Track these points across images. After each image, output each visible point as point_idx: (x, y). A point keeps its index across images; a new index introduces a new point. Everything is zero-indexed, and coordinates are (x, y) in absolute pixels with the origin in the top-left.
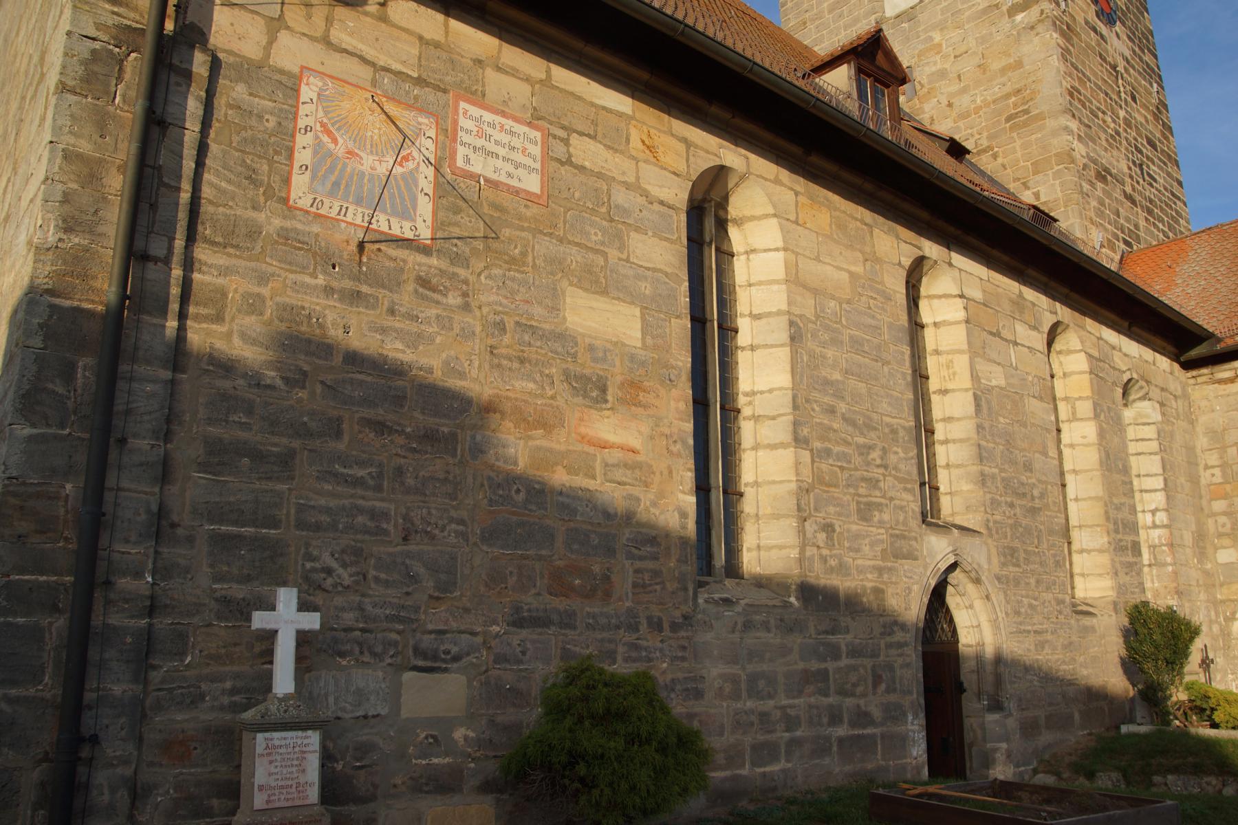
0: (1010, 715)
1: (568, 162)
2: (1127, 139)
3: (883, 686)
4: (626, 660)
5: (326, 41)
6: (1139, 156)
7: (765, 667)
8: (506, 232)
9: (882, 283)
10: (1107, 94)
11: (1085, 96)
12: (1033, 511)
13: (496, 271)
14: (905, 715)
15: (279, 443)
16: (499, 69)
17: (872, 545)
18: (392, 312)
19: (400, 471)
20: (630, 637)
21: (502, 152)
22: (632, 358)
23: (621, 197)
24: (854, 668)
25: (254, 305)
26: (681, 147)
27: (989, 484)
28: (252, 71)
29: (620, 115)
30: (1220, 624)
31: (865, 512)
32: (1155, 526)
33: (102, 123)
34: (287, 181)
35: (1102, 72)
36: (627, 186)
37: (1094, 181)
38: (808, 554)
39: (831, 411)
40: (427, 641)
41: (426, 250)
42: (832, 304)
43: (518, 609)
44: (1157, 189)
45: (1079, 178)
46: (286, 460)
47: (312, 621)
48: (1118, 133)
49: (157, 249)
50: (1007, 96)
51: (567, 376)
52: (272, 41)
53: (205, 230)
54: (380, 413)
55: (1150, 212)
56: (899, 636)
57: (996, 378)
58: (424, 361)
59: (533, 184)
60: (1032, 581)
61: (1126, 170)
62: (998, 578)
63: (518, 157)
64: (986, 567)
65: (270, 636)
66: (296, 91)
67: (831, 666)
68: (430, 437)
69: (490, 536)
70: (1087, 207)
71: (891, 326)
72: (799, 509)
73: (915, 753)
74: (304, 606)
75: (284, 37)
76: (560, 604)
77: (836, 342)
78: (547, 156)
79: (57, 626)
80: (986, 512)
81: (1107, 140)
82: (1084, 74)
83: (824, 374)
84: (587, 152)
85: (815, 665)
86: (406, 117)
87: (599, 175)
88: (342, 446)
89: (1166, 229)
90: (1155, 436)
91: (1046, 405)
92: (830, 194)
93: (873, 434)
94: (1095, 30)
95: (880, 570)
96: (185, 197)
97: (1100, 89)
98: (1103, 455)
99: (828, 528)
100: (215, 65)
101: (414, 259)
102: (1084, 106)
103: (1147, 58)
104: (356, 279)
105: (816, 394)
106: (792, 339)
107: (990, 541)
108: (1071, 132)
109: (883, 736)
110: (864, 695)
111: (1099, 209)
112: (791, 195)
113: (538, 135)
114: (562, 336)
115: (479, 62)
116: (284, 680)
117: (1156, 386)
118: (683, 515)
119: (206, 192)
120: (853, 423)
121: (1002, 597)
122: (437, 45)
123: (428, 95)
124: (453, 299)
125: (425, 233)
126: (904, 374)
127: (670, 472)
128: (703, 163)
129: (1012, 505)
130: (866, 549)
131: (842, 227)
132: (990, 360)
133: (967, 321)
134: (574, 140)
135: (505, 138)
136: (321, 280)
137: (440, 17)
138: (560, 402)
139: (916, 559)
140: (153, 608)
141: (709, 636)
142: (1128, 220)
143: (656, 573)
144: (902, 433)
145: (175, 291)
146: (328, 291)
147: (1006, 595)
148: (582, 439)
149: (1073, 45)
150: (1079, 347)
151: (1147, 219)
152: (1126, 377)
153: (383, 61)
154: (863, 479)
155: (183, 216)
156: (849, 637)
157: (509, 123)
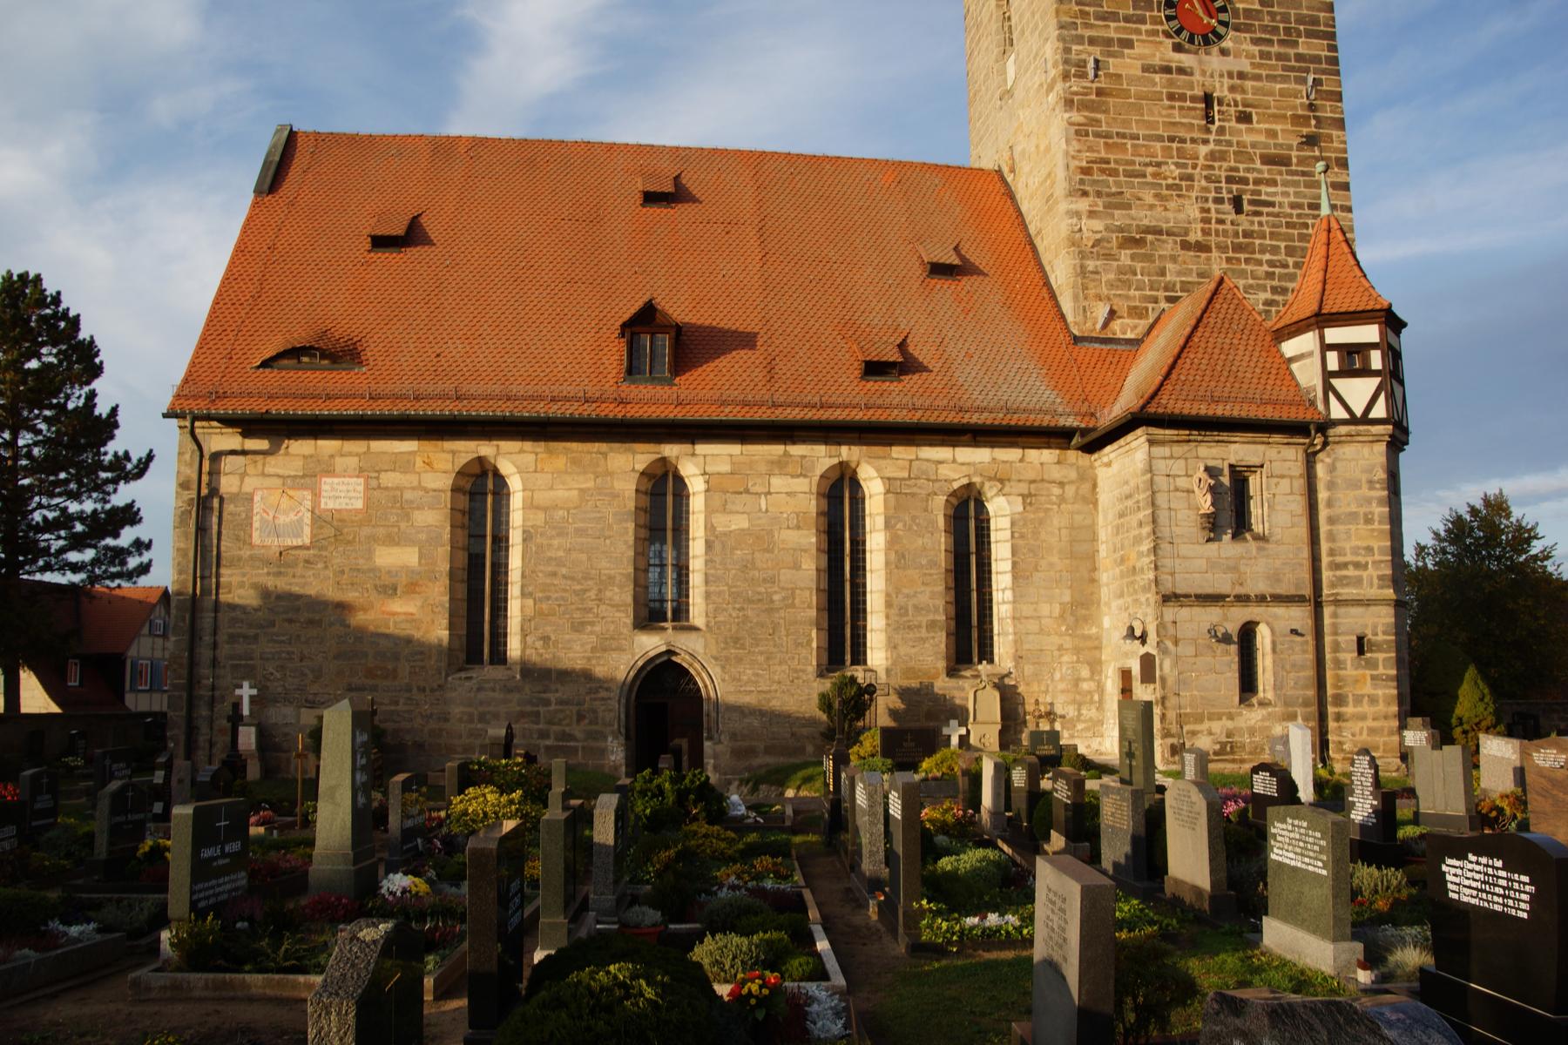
0: (720, 742)
1: (379, 487)
2: (1207, 178)
3: (587, 721)
4: (405, 704)
5: (263, 475)
6: (1234, 187)
7: (491, 709)
8: (345, 530)
9: (612, 487)
10: (1171, 139)
11: (1116, 162)
12: (770, 611)
13: (341, 549)
14: (605, 738)
15: (252, 632)
16: (342, 455)
17: (582, 645)
18: (294, 576)
19: (298, 636)
20: (408, 695)
21: (343, 495)
22: (413, 572)
23: (408, 495)
24: (562, 711)
25: (241, 585)
26: (450, 457)
27: (714, 598)
28: (235, 497)
29: (410, 453)
30: (1099, 682)
31: (578, 627)
32: (1004, 602)
33: (186, 535)
34: (251, 536)
35: (1169, 116)
36: (413, 489)
37: (1115, 251)
38: (528, 652)
39: (554, 574)
40: (310, 697)
41: (308, 548)
42: (561, 512)
43: (350, 685)
44: (1268, 214)
45: (1083, 258)
46: (256, 637)
47: (254, 692)
48: (1190, 178)
49: (207, 574)
50: (1045, 180)
51: (376, 586)
52: (242, 481)
53: (223, 562)
54: (290, 615)
55: (1238, 248)
56: (603, 694)
57: (739, 523)
58: (308, 593)
59: (359, 504)
60: (761, 659)
61: (1198, 215)
62: (716, 659)
63: (352, 494)
64: (702, 651)
65: (241, 697)
66: (252, 499)
67: (542, 709)
68: (311, 622)
69: (336, 657)
70: (1091, 285)
71: (615, 514)
72: (522, 629)
73: (613, 758)
74: (251, 687)
75: (247, 479)
76: (370, 682)
77: (562, 534)
78: (367, 488)
79: (185, 695)
80: (707, 615)
81: (1156, 196)
82: (1123, 136)
83: (549, 554)
84: (389, 479)
85: (529, 708)
86: (297, 494)
87: (397, 488)
88: (275, 630)
89: (1282, 257)
90: (1009, 526)
91: (805, 532)
92: (568, 445)
93: (590, 582)
94: (1167, 70)
95: (589, 659)
96: (215, 553)
97: (1160, 138)
98: (893, 556)
99: (546, 639)
100: (222, 500)
101: (303, 554)
102: (1114, 173)
103: (1305, 46)
104: (279, 567)
105: (542, 568)
106: (524, 540)
107: (708, 635)
108: (1078, 214)
109: (583, 748)
110: (568, 725)
111: (1120, 280)
112: (532, 457)
113: (361, 480)
114: (374, 570)
115: (332, 456)
116: (246, 711)
117: (1020, 481)
118: (440, 640)
119: (223, 548)
120: (572, 579)
121: (718, 669)
122: (311, 456)
123: (308, 480)
124: (320, 565)
125: (307, 541)
126: (626, 542)
127: (433, 622)
128: (463, 460)
129: (740, 610)
130: (577, 647)
131: (575, 462)
132: (731, 512)
133: (707, 491)
134: (383, 475)
135: (344, 488)
136: (266, 570)
137: (313, 442)
138: (372, 598)
139: (624, 650)
140: (213, 688)
141: (454, 694)
142: (1179, 273)
143: (423, 667)
144: (618, 578)
145: (214, 586)
146: (268, 574)
147: (723, 668)
148: (383, 613)
149: (1106, 112)
150: (875, 474)
151: (1229, 260)
152: (956, 485)
153: (287, 473)
154: (578, 609)
155: (214, 560)
156: (557, 695)
157: (346, 480)
